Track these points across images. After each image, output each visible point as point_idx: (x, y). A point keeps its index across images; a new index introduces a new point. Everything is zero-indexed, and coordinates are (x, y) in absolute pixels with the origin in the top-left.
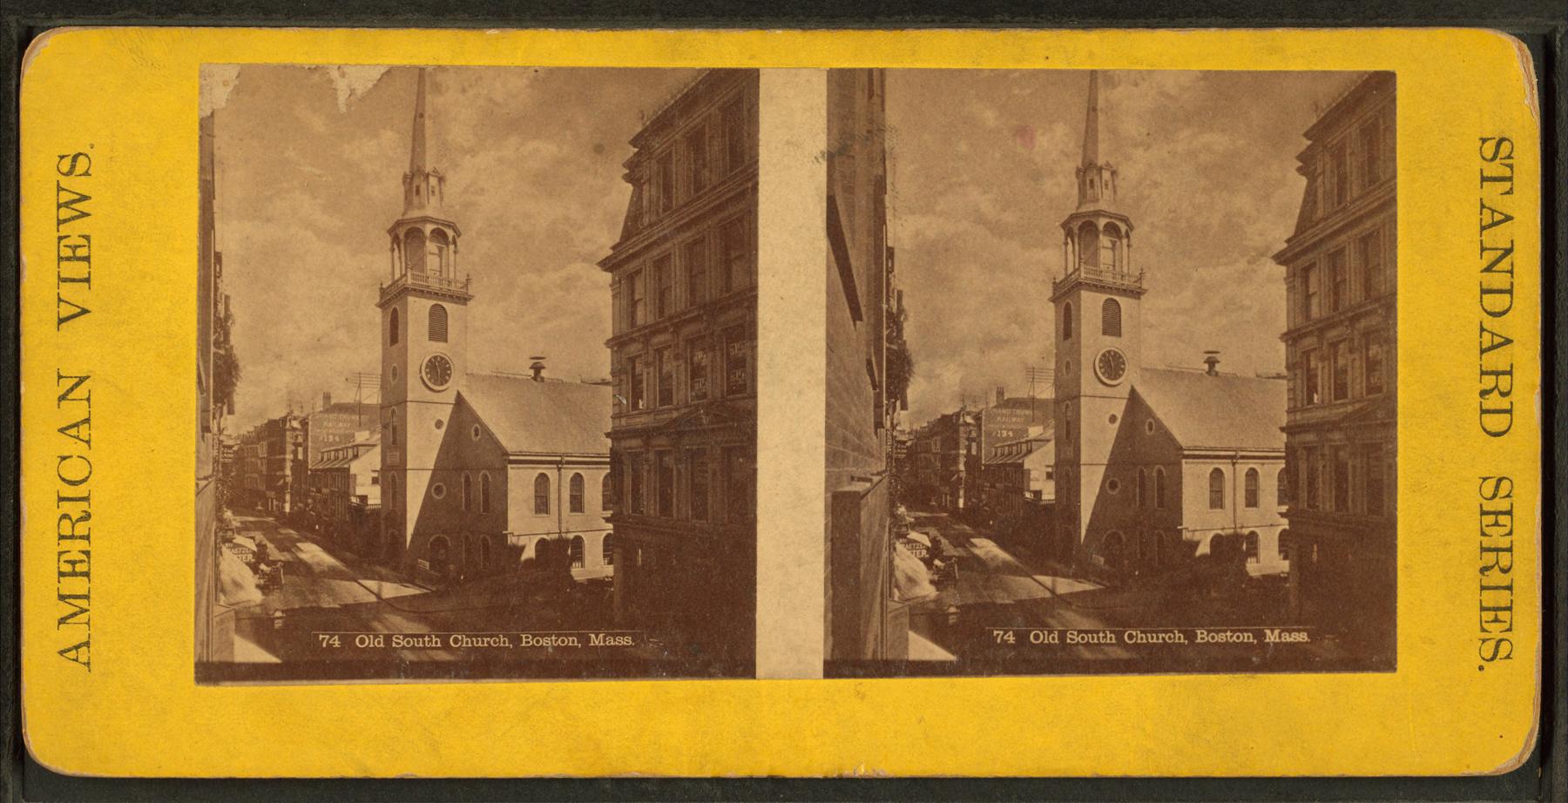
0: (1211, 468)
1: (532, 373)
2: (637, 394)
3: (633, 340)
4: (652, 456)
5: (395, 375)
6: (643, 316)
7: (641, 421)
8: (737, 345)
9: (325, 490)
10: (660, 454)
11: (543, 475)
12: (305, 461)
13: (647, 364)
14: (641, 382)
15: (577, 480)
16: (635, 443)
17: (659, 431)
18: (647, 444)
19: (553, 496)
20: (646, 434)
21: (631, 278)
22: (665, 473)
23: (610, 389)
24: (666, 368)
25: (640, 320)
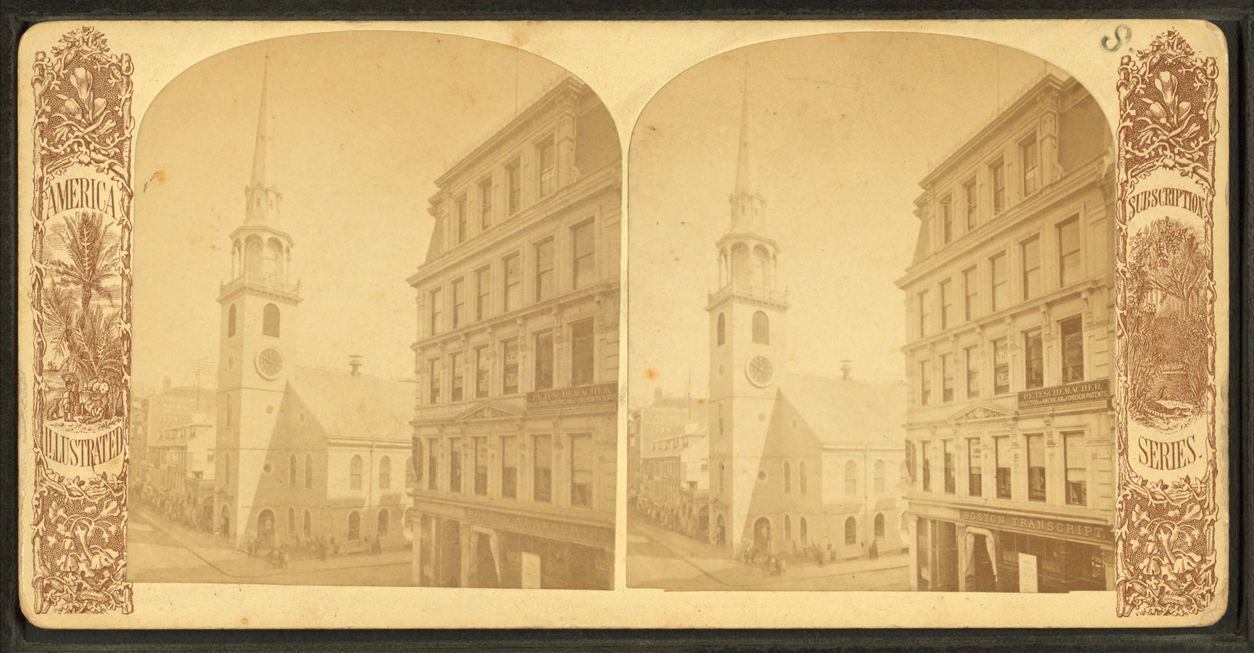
0: (847, 459)
1: (350, 369)
2: (435, 392)
3: (435, 345)
4: (446, 441)
5: (721, 371)
6: (443, 326)
7: (441, 413)
8: (512, 354)
9: (656, 478)
10: (452, 440)
11: (358, 457)
12: (639, 452)
13: (444, 367)
14: (438, 380)
15: (386, 460)
16: (433, 431)
17: (452, 422)
18: (441, 431)
19: (365, 477)
20: (443, 424)
21: (433, 293)
22: (455, 456)
23: (414, 385)
24: (457, 370)
25: (929, 330)
